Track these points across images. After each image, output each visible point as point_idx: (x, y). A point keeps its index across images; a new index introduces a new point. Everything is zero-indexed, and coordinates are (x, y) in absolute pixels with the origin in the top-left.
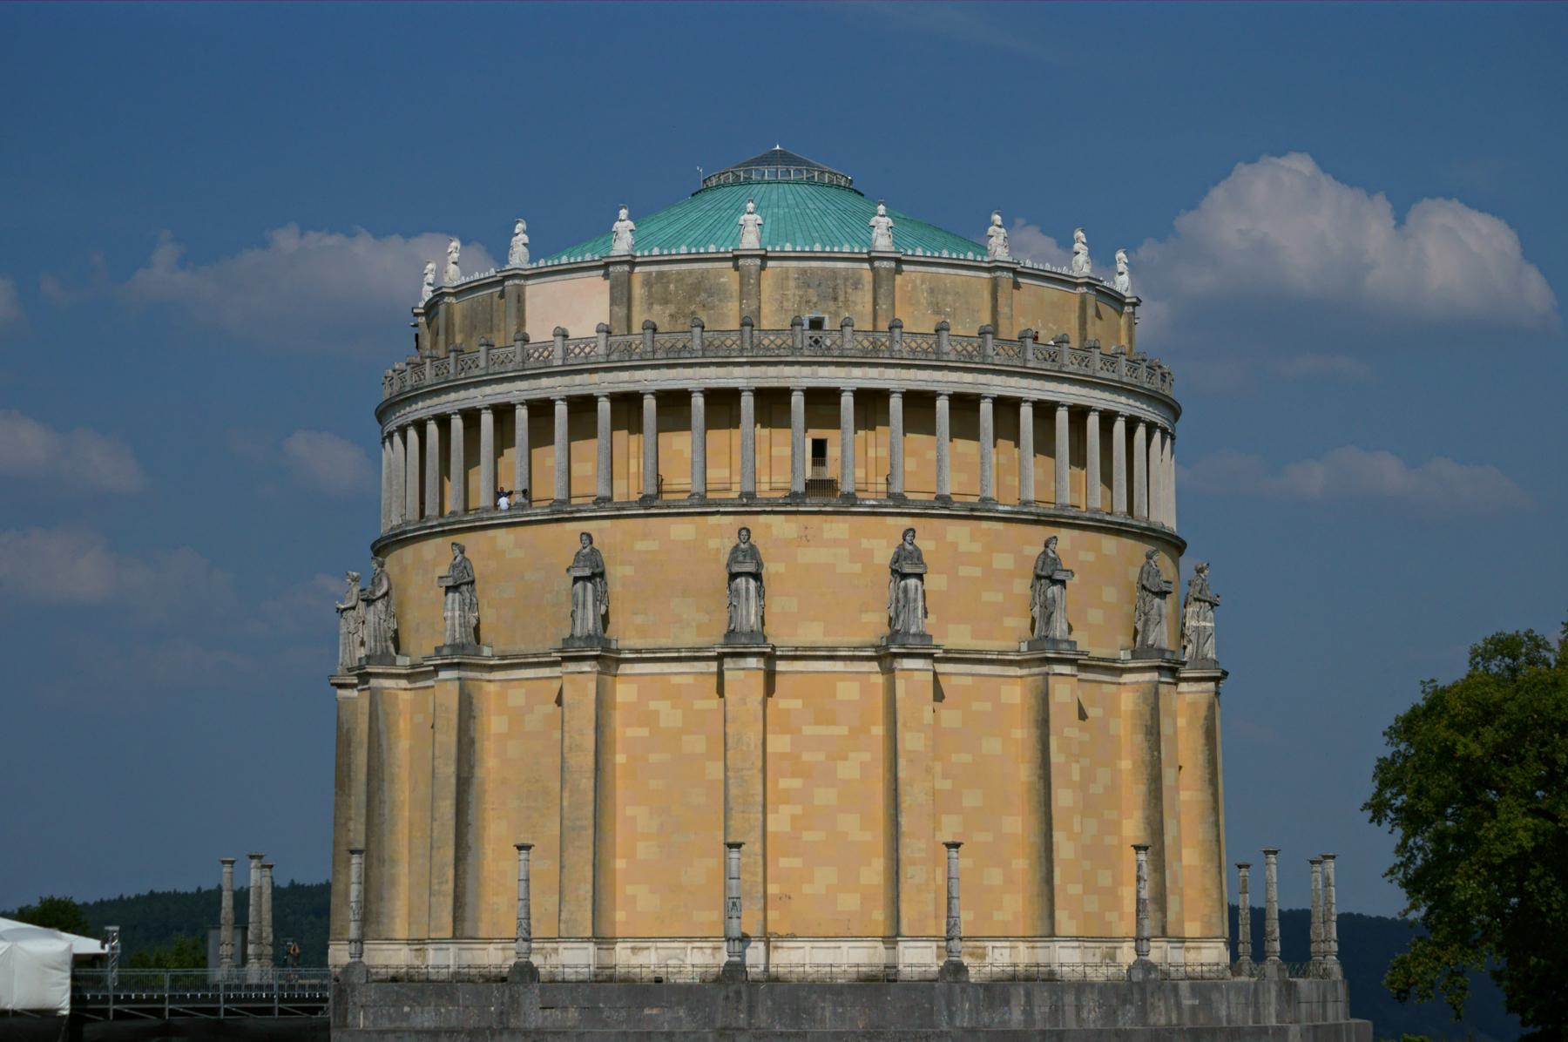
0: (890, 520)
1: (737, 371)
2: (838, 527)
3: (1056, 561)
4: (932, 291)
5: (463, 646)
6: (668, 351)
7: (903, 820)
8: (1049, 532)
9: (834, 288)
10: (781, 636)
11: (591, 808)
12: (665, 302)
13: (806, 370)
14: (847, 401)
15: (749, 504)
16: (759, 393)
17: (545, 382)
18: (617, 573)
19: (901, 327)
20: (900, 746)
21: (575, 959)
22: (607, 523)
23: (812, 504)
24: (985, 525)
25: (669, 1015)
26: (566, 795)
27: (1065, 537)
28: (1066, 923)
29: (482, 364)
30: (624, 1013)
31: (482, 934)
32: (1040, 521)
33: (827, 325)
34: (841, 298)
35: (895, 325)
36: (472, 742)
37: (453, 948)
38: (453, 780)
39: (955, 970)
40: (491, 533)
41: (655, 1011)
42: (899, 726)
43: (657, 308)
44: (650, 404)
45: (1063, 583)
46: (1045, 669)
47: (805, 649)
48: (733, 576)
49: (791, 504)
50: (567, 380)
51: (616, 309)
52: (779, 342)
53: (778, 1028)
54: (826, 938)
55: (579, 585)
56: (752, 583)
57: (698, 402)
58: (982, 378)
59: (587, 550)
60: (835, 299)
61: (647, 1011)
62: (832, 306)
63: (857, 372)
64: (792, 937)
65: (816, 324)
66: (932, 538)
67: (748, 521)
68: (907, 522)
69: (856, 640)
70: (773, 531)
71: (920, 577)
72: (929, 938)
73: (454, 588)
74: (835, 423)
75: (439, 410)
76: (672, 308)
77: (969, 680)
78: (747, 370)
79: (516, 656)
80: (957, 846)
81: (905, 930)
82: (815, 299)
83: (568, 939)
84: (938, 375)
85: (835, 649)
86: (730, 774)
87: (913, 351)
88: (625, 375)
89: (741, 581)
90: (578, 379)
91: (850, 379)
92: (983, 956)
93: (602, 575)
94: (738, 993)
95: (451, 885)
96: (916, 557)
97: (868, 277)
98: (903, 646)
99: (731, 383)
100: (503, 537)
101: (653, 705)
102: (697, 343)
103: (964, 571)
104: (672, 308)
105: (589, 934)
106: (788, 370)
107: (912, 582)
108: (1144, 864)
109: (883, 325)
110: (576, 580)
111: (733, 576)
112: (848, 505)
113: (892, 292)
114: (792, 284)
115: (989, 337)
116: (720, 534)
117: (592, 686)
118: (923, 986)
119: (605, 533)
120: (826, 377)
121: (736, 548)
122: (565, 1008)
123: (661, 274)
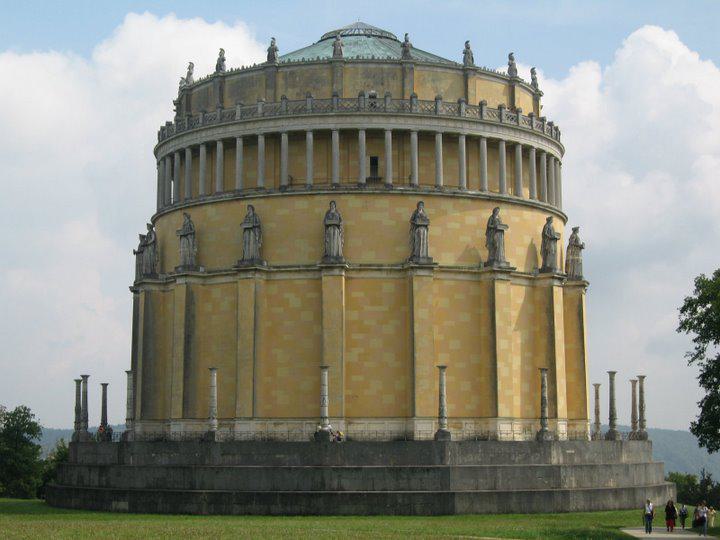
0: (411, 198)
1: (330, 120)
2: (383, 202)
5: (189, 267)
6: (294, 111)
7: (417, 355)
8: (496, 205)
9: (382, 79)
11: (251, 349)
12: (294, 86)
13: (366, 119)
14: (389, 136)
15: (336, 189)
17: (231, 129)
18: (269, 226)
19: (416, 97)
20: (415, 317)
21: (246, 429)
22: (262, 201)
23: (370, 189)
24: (461, 201)
26: (239, 342)
28: (503, 410)
29: (201, 121)
31: (198, 416)
32: (490, 199)
34: (386, 83)
35: (414, 96)
36: (193, 316)
37: (183, 424)
38: (183, 336)
39: (442, 434)
40: (204, 208)
41: (282, 456)
42: (415, 305)
43: (290, 90)
44: (285, 138)
46: (493, 275)
47: (365, 265)
48: (327, 226)
49: (358, 189)
50: (242, 127)
51: (268, 91)
52: (352, 105)
55: (247, 232)
56: (337, 231)
57: (310, 136)
59: (251, 214)
60: (382, 84)
61: (278, 456)
63: (393, 120)
64: (359, 418)
65: (372, 97)
67: (335, 198)
68: (420, 199)
69: (394, 261)
70: (350, 204)
72: (430, 418)
73: (185, 236)
74: (383, 149)
76: (297, 90)
77: (452, 283)
78: (335, 120)
79: (216, 271)
81: (418, 413)
82: (372, 84)
83: (240, 418)
84: (435, 122)
85: (382, 265)
86: (325, 331)
87: (423, 110)
88: (272, 124)
89: (331, 229)
90: (248, 126)
91: (389, 124)
93: (259, 227)
94: (326, 446)
95: (182, 391)
97: (399, 74)
98: (416, 263)
99: (326, 126)
100: (210, 210)
101: (286, 296)
102: (309, 106)
104: (297, 90)
105: (251, 416)
106: (357, 120)
107: (422, 230)
108: (546, 379)
109: (407, 97)
110: (245, 229)
111: (327, 226)
112: (387, 190)
113: (412, 80)
114: (360, 76)
116: (319, 206)
117: (253, 285)
118: (426, 443)
119: (262, 206)
120: (377, 123)
121: (329, 212)
122: (234, 455)
123: (292, 73)
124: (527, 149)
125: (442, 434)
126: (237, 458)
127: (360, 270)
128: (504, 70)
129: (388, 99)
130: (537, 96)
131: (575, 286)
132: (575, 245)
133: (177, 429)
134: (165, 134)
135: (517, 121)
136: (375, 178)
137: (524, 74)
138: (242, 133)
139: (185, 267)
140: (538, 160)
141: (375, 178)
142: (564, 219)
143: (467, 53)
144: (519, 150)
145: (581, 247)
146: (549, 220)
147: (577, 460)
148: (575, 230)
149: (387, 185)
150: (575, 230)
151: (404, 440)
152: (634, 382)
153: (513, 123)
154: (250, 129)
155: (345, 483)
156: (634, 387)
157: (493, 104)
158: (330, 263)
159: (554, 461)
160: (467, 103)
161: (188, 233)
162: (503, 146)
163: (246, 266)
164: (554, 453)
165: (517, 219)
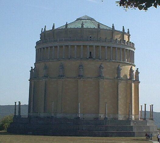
23: (89, 60)
33: (92, 37)
65: (90, 37)
75: (43, 47)
99: (80, 44)
125: (106, 118)
128: (121, 30)
130: (129, 36)
131: (137, 83)
132: (137, 72)
133: (42, 115)
134: (37, 43)
137: (126, 31)
138: (59, 45)
139: (45, 76)
140: (129, 52)
142: (135, 66)
143: (113, 26)
144: (125, 50)
145: (139, 73)
148: (138, 69)
149: (94, 59)
150: (138, 69)
151: (97, 119)
152: (150, 106)
154: (61, 44)
156: (151, 107)
158: (80, 76)
160: (113, 39)
161: (46, 68)
163: (61, 76)
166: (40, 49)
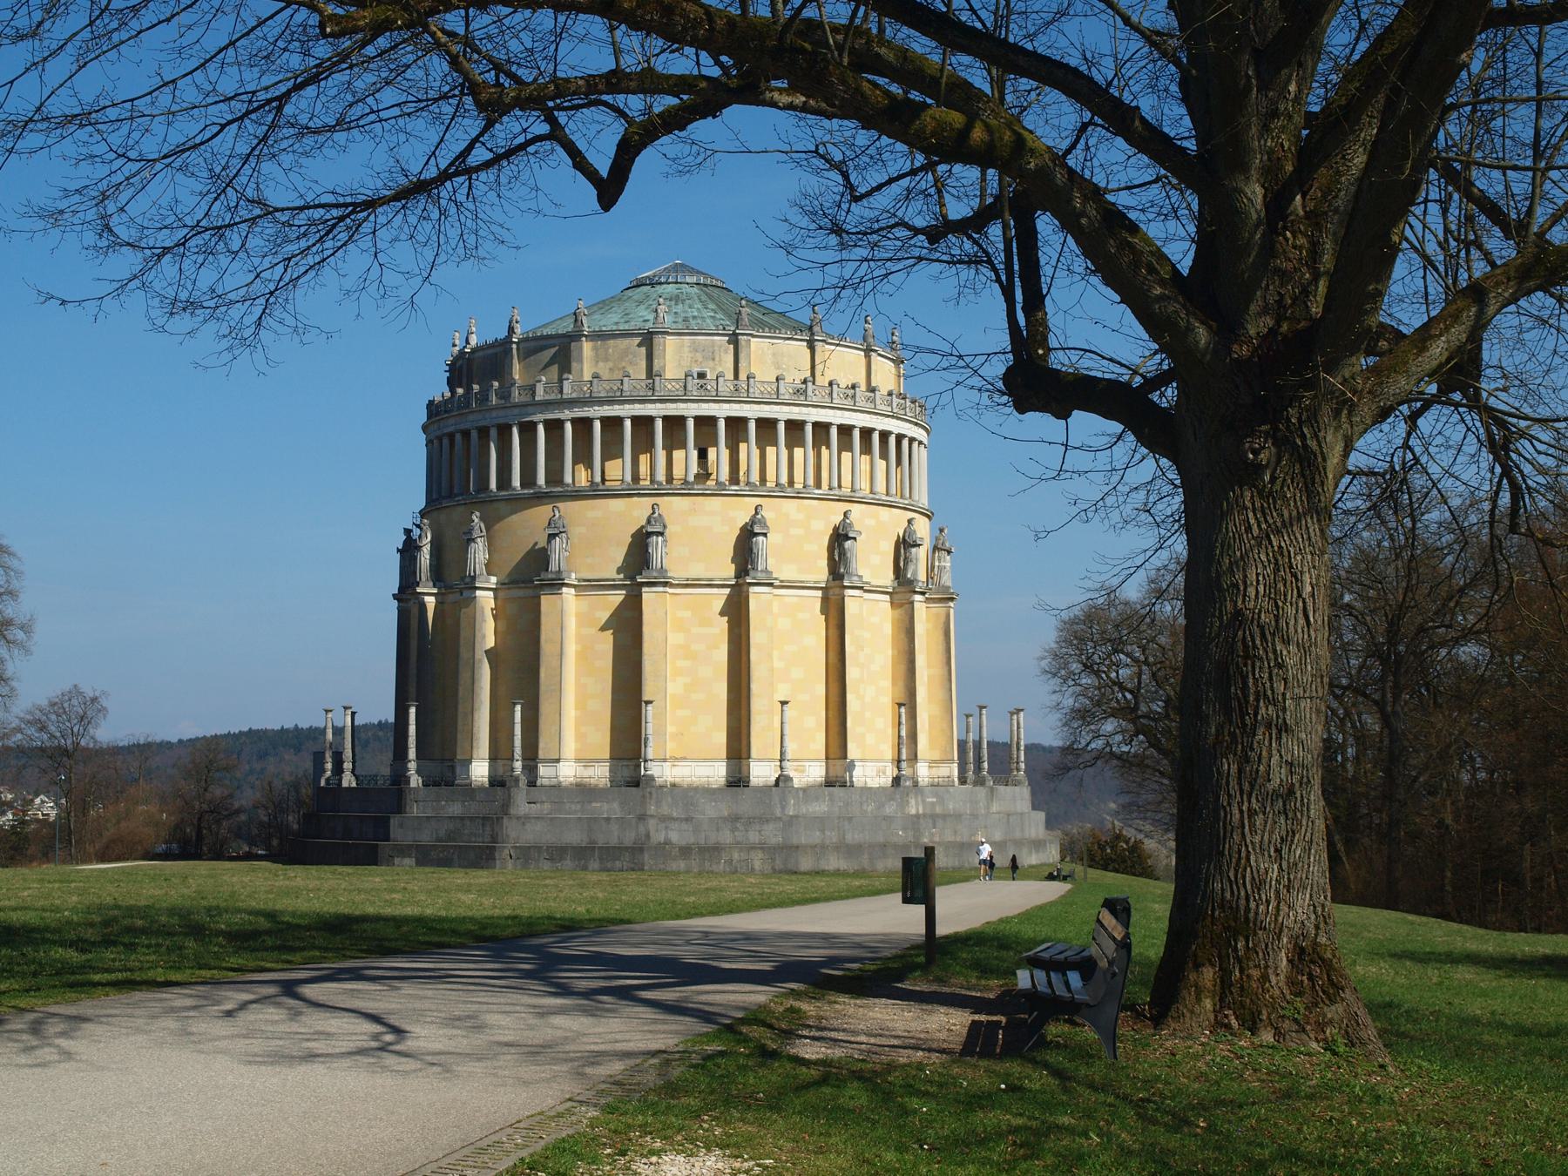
3: (851, 525)
4: (774, 355)
8: (847, 506)
10: (676, 572)
12: (606, 360)
15: (656, 491)
16: (666, 419)
23: (698, 488)
25: (606, 807)
27: (856, 510)
30: (579, 806)
39: (782, 781)
43: (601, 364)
45: (855, 539)
49: (686, 489)
53: (675, 814)
54: (705, 760)
58: (804, 410)
62: (711, 363)
65: (702, 376)
66: (776, 512)
68: (758, 501)
70: (672, 507)
71: (765, 535)
75: (462, 427)
76: (610, 364)
80: (786, 703)
87: (762, 393)
92: (803, 771)
96: (763, 523)
103: (793, 531)
104: (610, 364)
107: (761, 538)
113: (749, 355)
114: (686, 349)
115: (810, 384)
124: (884, 435)
125: (782, 781)
126: (547, 806)
127: (687, 586)
129: (721, 380)
135: (874, 401)
136: (704, 475)
141: (704, 475)
146: (910, 521)
147: (938, 810)
153: (869, 405)
155: (674, 837)
157: (844, 382)
159: (913, 812)
162: (856, 433)
164: (913, 802)
165: (871, 522)
166: (446, 441)
